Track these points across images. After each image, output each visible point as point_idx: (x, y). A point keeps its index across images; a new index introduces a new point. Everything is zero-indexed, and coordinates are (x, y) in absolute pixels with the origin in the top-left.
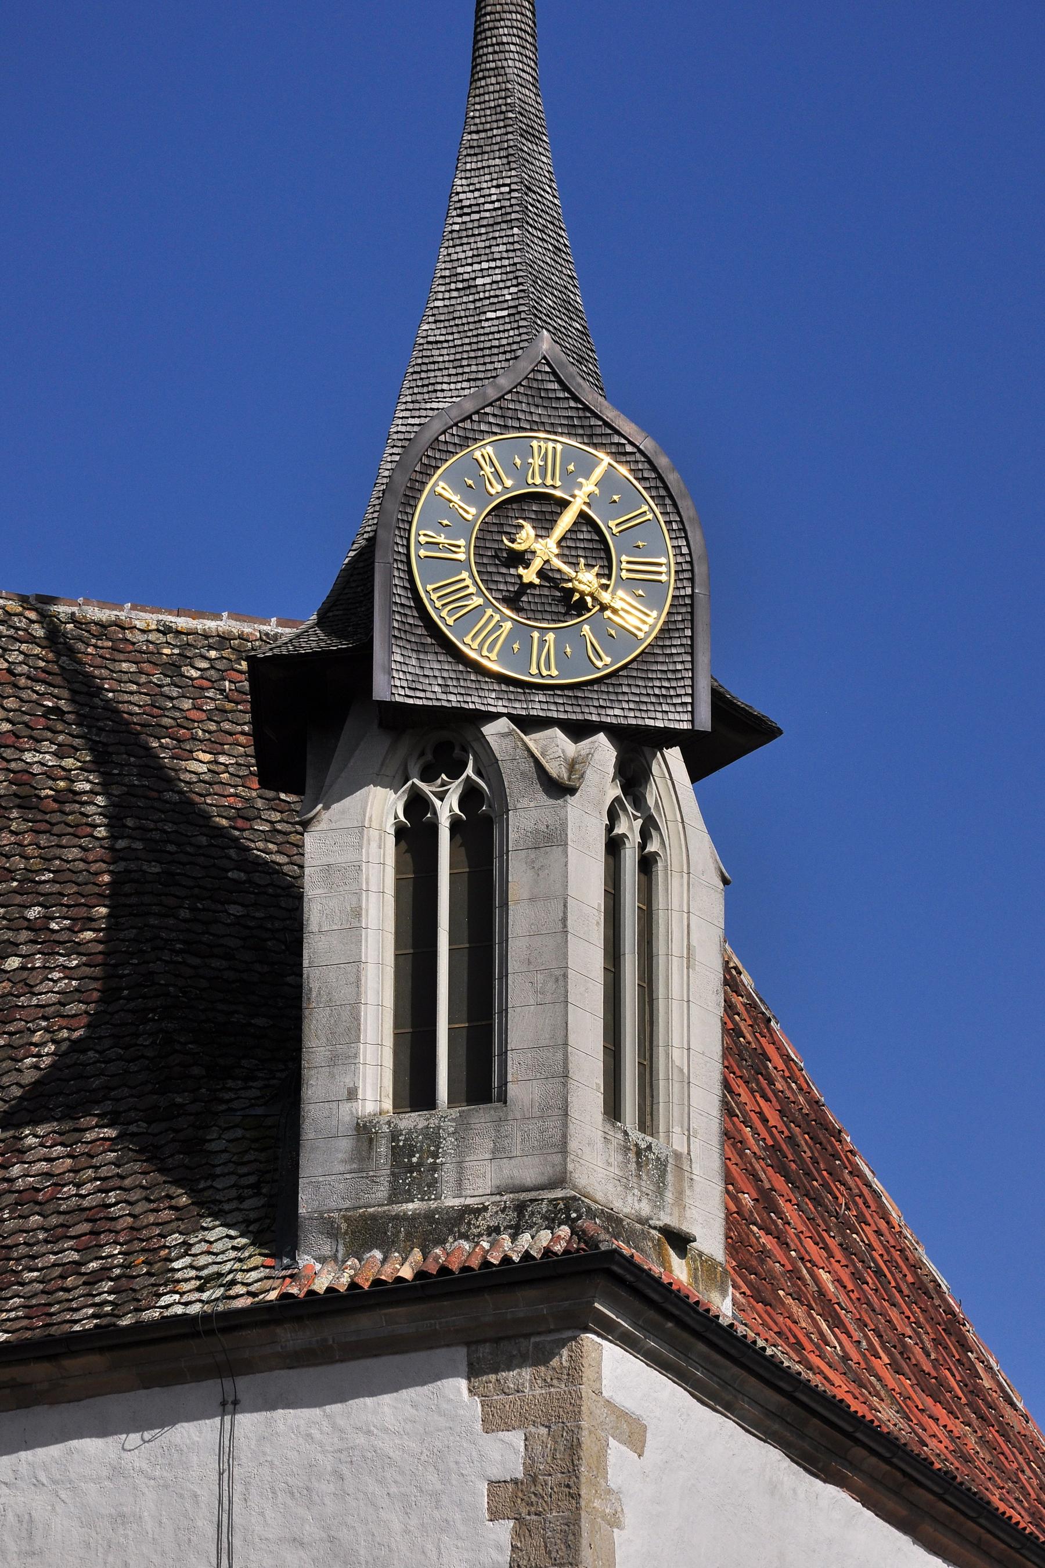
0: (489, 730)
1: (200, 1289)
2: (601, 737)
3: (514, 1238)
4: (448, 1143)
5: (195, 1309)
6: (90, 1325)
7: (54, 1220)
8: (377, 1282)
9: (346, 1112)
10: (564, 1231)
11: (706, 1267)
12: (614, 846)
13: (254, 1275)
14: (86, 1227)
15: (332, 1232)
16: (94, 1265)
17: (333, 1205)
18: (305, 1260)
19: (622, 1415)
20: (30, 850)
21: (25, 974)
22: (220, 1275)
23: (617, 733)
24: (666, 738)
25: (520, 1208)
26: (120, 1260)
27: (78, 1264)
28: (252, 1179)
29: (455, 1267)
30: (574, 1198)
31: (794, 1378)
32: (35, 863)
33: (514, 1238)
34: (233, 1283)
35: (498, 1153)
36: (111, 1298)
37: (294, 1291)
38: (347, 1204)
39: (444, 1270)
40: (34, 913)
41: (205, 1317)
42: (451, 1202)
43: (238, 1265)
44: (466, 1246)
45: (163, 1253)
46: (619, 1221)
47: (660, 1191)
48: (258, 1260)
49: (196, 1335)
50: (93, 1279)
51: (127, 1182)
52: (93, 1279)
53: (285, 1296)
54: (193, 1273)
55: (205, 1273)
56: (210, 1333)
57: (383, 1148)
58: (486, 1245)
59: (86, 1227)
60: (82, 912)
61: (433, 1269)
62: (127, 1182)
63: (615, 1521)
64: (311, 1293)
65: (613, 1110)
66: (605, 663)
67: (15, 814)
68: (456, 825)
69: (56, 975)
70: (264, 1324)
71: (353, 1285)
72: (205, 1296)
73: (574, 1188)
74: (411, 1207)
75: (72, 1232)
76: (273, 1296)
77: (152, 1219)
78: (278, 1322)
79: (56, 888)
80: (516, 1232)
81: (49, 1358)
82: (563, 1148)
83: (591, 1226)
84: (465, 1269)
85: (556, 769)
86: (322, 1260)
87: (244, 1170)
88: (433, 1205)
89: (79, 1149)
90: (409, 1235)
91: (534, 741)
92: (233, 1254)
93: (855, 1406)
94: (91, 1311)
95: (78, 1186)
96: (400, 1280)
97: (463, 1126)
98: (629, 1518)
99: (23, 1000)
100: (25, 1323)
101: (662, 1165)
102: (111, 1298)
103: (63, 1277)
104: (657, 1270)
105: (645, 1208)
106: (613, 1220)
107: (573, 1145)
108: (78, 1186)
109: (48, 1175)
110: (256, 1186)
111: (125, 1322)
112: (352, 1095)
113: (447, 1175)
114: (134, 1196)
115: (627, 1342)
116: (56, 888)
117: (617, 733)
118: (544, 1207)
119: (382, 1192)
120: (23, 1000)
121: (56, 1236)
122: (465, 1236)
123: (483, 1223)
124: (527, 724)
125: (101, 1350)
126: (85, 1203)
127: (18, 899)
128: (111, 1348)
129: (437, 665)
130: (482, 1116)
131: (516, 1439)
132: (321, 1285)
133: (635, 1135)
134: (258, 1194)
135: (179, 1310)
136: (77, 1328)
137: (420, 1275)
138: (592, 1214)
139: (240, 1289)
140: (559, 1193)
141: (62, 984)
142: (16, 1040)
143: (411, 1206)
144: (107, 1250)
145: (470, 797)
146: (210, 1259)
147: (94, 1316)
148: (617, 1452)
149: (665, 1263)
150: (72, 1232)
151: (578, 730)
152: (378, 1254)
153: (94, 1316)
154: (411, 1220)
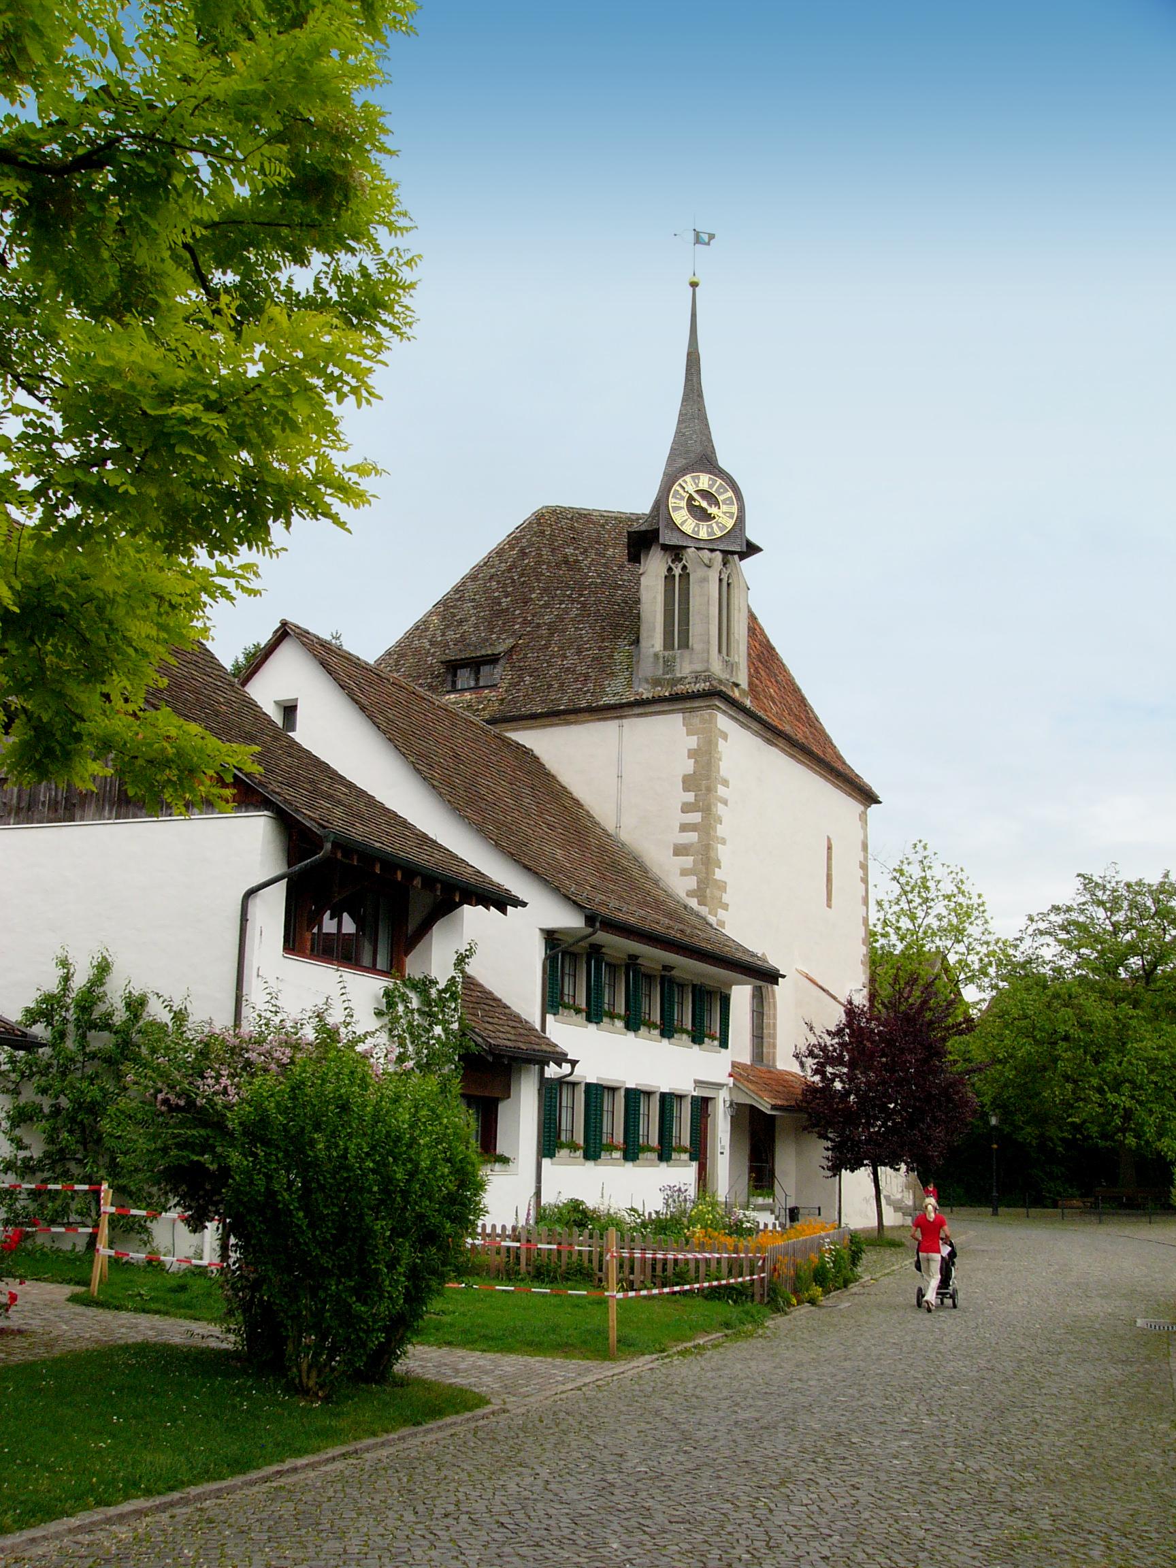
0: (689, 550)
2: (718, 552)
4: (678, 660)
9: (652, 651)
10: (708, 684)
11: (743, 692)
12: (720, 580)
15: (647, 681)
19: (722, 732)
23: (721, 551)
24: (733, 553)
31: (766, 722)
35: (691, 663)
47: (732, 671)
57: (661, 660)
61: (673, 693)
63: (720, 759)
65: (720, 651)
66: (719, 534)
68: (680, 575)
74: (668, 677)
80: (696, 683)
83: (714, 682)
85: (707, 561)
91: (701, 553)
93: (780, 727)
97: (682, 656)
98: (723, 759)
101: (732, 665)
104: (731, 694)
105: (728, 677)
106: (720, 682)
112: (653, 646)
113: (677, 668)
115: (724, 712)
117: (721, 551)
119: (661, 672)
121: (576, 680)
123: (687, 681)
124: (698, 549)
129: (676, 534)
130: (686, 653)
131: (695, 738)
133: (726, 658)
138: (715, 679)
145: (684, 568)
148: (721, 741)
149: (733, 691)
151: (712, 550)
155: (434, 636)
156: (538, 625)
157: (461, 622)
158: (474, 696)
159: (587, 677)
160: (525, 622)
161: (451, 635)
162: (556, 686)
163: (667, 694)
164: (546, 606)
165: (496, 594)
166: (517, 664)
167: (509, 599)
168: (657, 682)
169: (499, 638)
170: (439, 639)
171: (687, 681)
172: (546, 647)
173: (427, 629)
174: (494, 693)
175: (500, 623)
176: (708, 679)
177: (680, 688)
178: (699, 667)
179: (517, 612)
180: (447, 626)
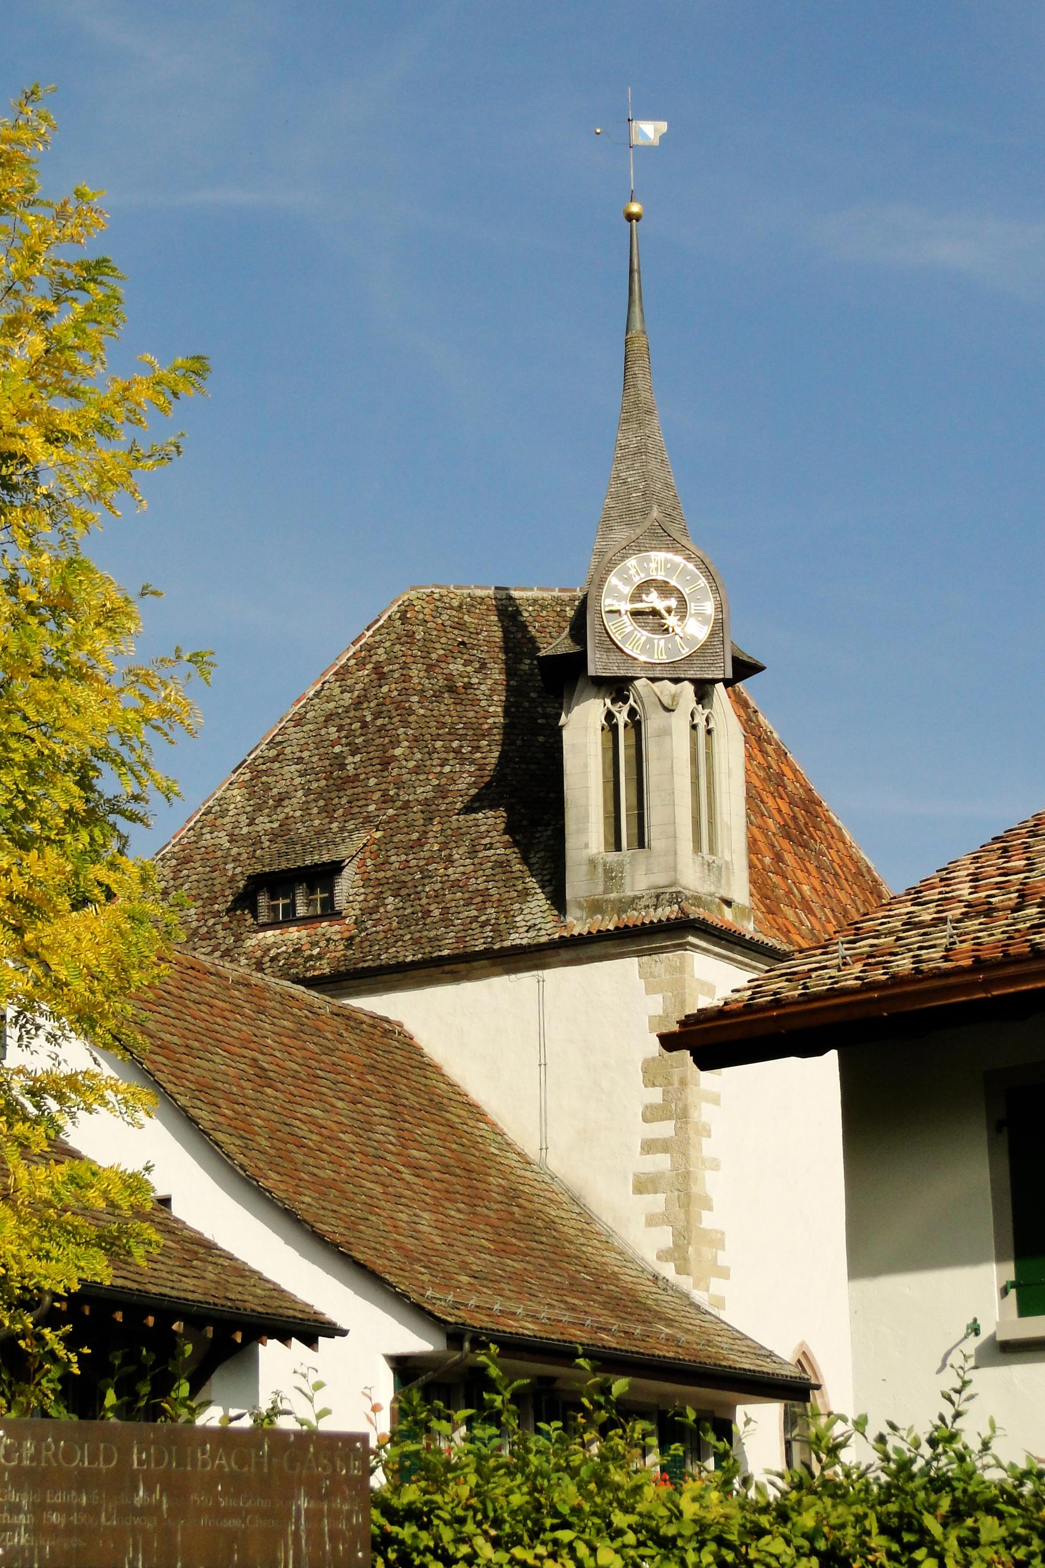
1: (527, 931)
3: (655, 909)
5: (525, 942)
6: (482, 947)
7: (467, 895)
8: (599, 931)
13: (549, 925)
14: (480, 899)
15: (580, 906)
16: (483, 918)
17: (580, 895)
18: (569, 919)
20: (453, 713)
21: (452, 774)
22: (535, 925)
25: (658, 897)
26: (494, 916)
27: (477, 917)
28: (548, 877)
29: (631, 925)
30: (679, 892)
32: (455, 719)
33: (655, 909)
34: (540, 929)
36: (491, 934)
37: (565, 934)
38: (586, 894)
39: (626, 926)
40: (456, 744)
41: (529, 946)
42: (629, 893)
43: (542, 920)
44: (636, 913)
45: (512, 913)
46: (700, 898)
48: (550, 918)
49: (526, 953)
50: (484, 925)
51: (497, 878)
52: (484, 925)
53: (561, 937)
54: (524, 923)
55: (529, 924)
56: (530, 952)
58: (643, 914)
59: (480, 899)
60: (475, 743)
62: (497, 878)
64: (572, 936)
67: (446, 695)
69: (465, 775)
70: (553, 948)
71: (589, 933)
72: (529, 935)
73: (681, 886)
74: (613, 896)
75: (474, 901)
76: (556, 936)
77: (507, 895)
78: (560, 947)
79: (464, 732)
81: (467, 962)
82: (675, 869)
84: (635, 926)
86: (577, 919)
87: (545, 872)
88: (622, 895)
89: (476, 861)
90: (612, 909)
92: (540, 914)
94: (482, 941)
95: (477, 879)
96: (608, 930)
99: (451, 788)
100: (456, 945)
102: (491, 934)
103: (471, 923)
107: (679, 867)
108: (477, 879)
109: (464, 873)
110: (549, 881)
111: (496, 947)
114: (500, 884)
116: (464, 732)
118: (667, 896)
120: (451, 788)
122: (634, 909)
123: (643, 903)
125: (488, 959)
126: (480, 887)
127: (449, 737)
128: (491, 958)
132: (576, 932)
134: (551, 885)
135: (518, 942)
136: (477, 949)
137: (617, 928)
139: (543, 932)
140: (673, 890)
141: (468, 780)
142: (449, 807)
143: (612, 895)
144: (489, 911)
146: (531, 916)
147: (484, 943)
150: (474, 901)
152: (599, 917)
153: (484, 943)
154: (613, 902)
155: (236, 824)
156: (406, 805)
157: (280, 801)
158: (304, 933)
159: (484, 893)
160: (387, 800)
161: (264, 825)
162: (436, 913)
163: (611, 927)
164: (417, 770)
165: (337, 749)
166: (373, 875)
167: (358, 758)
168: (596, 907)
169: (342, 829)
170: (245, 830)
171: (643, 903)
172: (420, 843)
173: (223, 814)
174: (337, 928)
175: (344, 801)
176: (676, 898)
177: (633, 917)
178: (661, 879)
179: (372, 782)
180: (258, 808)
